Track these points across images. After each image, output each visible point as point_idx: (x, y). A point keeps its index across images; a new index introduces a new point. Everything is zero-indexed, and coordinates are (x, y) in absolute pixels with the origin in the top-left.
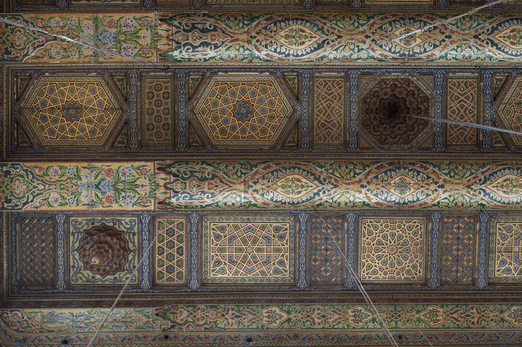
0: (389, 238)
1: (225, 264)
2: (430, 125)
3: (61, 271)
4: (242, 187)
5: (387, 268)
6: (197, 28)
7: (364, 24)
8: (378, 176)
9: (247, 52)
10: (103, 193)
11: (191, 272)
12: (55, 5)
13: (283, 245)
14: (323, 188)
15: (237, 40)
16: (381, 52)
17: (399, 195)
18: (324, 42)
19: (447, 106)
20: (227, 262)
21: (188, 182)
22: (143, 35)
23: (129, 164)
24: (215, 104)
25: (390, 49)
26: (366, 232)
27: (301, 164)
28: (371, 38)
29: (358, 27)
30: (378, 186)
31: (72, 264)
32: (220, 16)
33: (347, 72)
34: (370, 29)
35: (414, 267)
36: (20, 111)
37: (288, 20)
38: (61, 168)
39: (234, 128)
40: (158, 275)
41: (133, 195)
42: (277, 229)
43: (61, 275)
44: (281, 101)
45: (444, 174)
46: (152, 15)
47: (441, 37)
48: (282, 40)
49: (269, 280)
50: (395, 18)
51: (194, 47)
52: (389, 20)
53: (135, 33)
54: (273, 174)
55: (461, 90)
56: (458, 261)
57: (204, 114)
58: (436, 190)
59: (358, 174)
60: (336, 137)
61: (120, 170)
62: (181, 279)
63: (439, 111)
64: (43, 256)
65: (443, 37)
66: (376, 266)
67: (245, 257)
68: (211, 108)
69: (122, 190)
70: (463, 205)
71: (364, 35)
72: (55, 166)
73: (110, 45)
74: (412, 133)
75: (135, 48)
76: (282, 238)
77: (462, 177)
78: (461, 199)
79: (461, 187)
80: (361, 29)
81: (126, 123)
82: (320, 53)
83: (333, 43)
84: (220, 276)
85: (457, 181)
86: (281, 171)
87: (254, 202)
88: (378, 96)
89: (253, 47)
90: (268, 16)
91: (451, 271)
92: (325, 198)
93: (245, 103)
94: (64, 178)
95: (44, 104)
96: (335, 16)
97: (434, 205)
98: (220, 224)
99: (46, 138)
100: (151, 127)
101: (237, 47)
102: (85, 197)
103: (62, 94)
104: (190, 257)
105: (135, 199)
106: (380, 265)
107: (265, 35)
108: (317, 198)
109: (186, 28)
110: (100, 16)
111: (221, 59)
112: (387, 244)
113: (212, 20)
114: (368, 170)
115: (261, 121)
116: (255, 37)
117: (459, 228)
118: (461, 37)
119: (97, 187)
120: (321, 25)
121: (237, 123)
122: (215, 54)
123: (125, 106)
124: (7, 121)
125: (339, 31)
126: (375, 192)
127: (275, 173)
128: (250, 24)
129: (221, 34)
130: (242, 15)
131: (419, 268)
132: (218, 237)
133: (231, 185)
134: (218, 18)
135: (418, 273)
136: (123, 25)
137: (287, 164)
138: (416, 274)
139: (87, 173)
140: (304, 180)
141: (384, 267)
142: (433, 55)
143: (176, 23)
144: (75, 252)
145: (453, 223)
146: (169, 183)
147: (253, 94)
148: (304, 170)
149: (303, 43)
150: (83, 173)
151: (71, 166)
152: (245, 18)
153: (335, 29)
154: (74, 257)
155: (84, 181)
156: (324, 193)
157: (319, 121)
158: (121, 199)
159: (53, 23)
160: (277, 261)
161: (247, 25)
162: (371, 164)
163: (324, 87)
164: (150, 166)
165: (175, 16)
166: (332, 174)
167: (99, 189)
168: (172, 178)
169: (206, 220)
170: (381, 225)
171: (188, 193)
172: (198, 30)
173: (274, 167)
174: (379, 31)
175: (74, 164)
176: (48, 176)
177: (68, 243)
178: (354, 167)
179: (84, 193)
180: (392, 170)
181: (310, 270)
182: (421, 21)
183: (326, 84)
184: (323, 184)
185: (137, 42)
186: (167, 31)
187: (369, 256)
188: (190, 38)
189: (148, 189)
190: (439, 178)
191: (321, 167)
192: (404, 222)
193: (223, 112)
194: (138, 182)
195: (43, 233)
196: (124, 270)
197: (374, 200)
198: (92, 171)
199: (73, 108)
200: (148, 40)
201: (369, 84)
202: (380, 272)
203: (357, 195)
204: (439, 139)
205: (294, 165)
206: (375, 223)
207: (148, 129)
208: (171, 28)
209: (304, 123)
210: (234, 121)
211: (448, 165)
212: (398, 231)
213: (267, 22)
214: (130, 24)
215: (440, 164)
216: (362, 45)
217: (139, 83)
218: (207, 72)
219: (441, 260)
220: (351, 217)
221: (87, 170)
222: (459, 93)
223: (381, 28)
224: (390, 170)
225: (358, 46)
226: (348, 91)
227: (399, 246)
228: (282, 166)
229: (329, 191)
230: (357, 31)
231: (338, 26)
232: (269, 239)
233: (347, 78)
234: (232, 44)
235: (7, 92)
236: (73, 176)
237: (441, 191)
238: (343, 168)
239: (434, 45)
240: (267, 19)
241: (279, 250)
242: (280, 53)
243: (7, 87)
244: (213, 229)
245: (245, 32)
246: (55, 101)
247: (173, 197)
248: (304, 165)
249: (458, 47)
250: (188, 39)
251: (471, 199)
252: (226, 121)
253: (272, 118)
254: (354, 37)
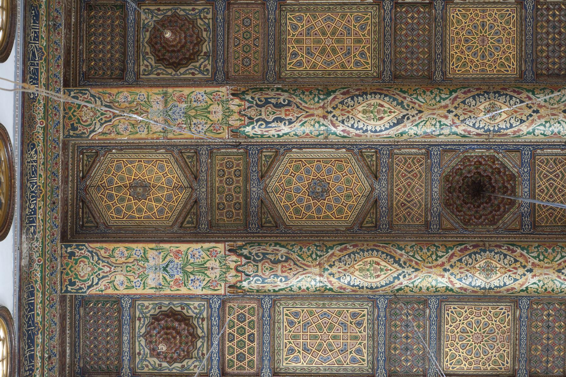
0: (474, 325)
1: (299, 352)
2: (517, 205)
3: (126, 358)
4: (317, 270)
5: (472, 358)
6: (270, 103)
7: (446, 98)
8: (461, 259)
9: (322, 128)
10: (171, 276)
11: (263, 360)
12: (123, 79)
13: (360, 332)
14: (404, 272)
15: (313, 115)
16: (464, 128)
17: (485, 280)
18: (404, 116)
19: (535, 184)
20: (301, 350)
21: (260, 265)
22: (214, 110)
23: (199, 246)
24: (289, 182)
25: (474, 125)
26: (449, 319)
27: (379, 246)
28: (454, 113)
29: (439, 102)
30: (462, 270)
31: (137, 351)
32: (294, 90)
33: (428, 149)
34: (453, 104)
35: (501, 357)
36: (86, 189)
37: (366, 94)
38: (128, 249)
39: (308, 208)
40: (228, 363)
41: (203, 278)
42: (354, 315)
43: (126, 362)
44: (358, 179)
45: (533, 257)
46: (223, 89)
47: (528, 112)
48: (360, 115)
49: (345, 369)
50: (479, 92)
51: (267, 123)
52: (472, 94)
53: (206, 109)
54: (349, 256)
55: (549, 167)
56: (548, 350)
57: (277, 193)
58: (525, 275)
59: (441, 257)
60: (417, 217)
61: (189, 251)
62: (252, 368)
63: (527, 190)
64: (108, 342)
65: (530, 111)
66: (460, 356)
67: (320, 345)
68: (285, 187)
69: (191, 273)
70: (553, 290)
71: (447, 109)
72: (122, 247)
73: (180, 121)
74: (498, 213)
75: (206, 123)
76: (359, 324)
77: (552, 261)
78: (551, 284)
79: (551, 271)
80: (443, 103)
81: (196, 202)
82: (400, 129)
83: (414, 118)
84: (294, 364)
85: (547, 265)
86: (358, 253)
87: (329, 286)
88: (461, 174)
89: (329, 123)
90: (345, 90)
91: (541, 362)
92: (405, 283)
93: (321, 181)
94: (131, 260)
95: (110, 182)
96: (415, 90)
97: (522, 291)
98: (294, 309)
99: (113, 217)
100: (221, 206)
101: (312, 123)
102: (153, 280)
103: (130, 171)
104: (262, 344)
105: (205, 282)
106: (465, 354)
107: (342, 110)
108: (397, 282)
109: (259, 103)
110: (170, 90)
111: (296, 135)
112: (472, 332)
113: (286, 95)
114: (451, 252)
115: (337, 200)
116: (331, 112)
117: (549, 315)
118: (549, 112)
119: (165, 269)
120: (400, 99)
121: (312, 202)
122: (289, 130)
123: (195, 185)
124: (72, 200)
125: (420, 106)
126: (458, 277)
127: (352, 256)
128: (326, 98)
129: (295, 109)
130: (317, 89)
131: (506, 358)
132: (291, 323)
133: (306, 268)
134: (292, 92)
135: (505, 363)
136: (193, 100)
137: (365, 246)
138: (503, 365)
139: (154, 254)
140: (383, 263)
141: (469, 357)
142: (519, 130)
143: (248, 97)
144: (141, 338)
145: (543, 309)
146: (240, 266)
147: (329, 171)
148: (383, 253)
149: (382, 118)
150: (151, 254)
151: (138, 247)
152: (321, 92)
153: (415, 103)
154: (140, 343)
155: (152, 263)
156: (404, 276)
157: (399, 201)
158: (190, 282)
159: (121, 98)
160: (354, 349)
161: (323, 100)
162: (454, 246)
163: (404, 164)
164: (220, 247)
165: (248, 91)
166: (413, 256)
167: (167, 271)
168: (244, 261)
169: (279, 304)
170: (466, 312)
171: (260, 277)
172: (271, 105)
173: (351, 249)
174: (462, 105)
175: (140, 246)
176: (114, 257)
177: (134, 328)
178: (436, 250)
179: (152, 275)
180: (477, 253)
181: (389, 359)
182: (507, 95)
183: (406, 161)
184: (403, 267)
185: (208, 118)
186: (239, 106)
187: (452, 345)
188: (263, 113)
189: (218, 272)
190: (527, 262)
191: (401, 249)
192: (490, 309)
193: (298, 190)
194: (208, 265)
195: (107, 318)
196: (192, 358)
197: (458, 285)
198: (160, 253)
199: (141, 186)
200: (220, 116)
201: (451, 162)
202: (464, 362)
203: (440, 279)
204: (527, 220)
205: (372, 247)
206: (459, 309)
207: (219, 209)
208: (243, 103)
209: (383, 202)
210: (308, 200)
211: (537, 247)
212: (484, 319)
213: (344, 96)
214: (201, 98)
215: (528, 247)
216: (444, 121)
217: (209, 160)
218: (280, 149)
219: (530, 350)
220: (433, 303)
221: (154, 251)
222: (547, 171)
223: (464, 102)
224: (475, 253)
225: (440, 122)
226: (430, 168)
227: (485, 334)
228: (359, 248)
229: (409, 275)
230: (438, 105)
231: (418, 100)
232: (345, 326)
233: (428, 154)
234: (307, 119)
235: (73, 169)
236: (139, 258)
237: (529, 275)
238: (425, 251)
239: (521, 120)
240: (343, 94)
241: (356, 338)
242: (357, 129)
243: (73, 164)
244: (287, 315)
245: (320, 107)
246: (122, 179)
247: (245, 281)
248: (383, 247)
249: (546, 122)
250: (261, 115)
251: (562, 284)
252: (300, 200)
253: (348, 197)
254: (435, 112)
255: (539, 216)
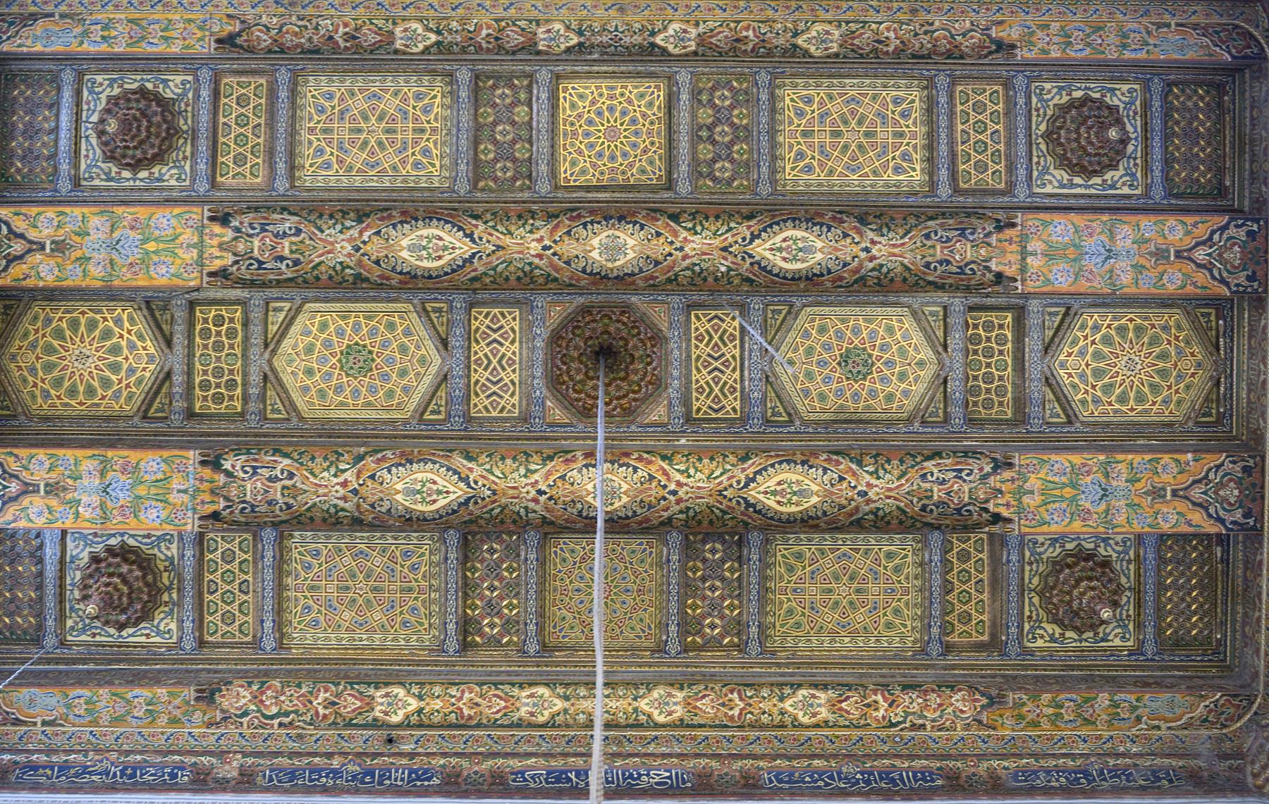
18: (474, 255)
45: (678, 470)
52: (583, 220)
190: (669, 479)
255: (488, 411)
